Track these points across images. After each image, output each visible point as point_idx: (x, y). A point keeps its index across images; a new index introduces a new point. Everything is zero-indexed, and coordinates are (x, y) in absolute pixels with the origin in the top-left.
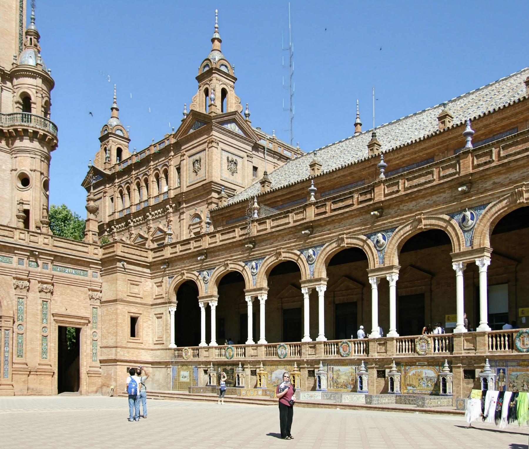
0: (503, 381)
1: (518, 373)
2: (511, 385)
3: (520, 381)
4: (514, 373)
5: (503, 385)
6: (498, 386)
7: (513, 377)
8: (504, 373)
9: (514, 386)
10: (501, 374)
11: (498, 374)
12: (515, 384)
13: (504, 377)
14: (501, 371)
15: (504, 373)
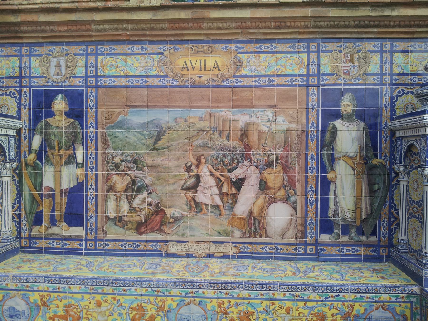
0: (71, 160)
1: (165, 117)
2: (120, 183)
3: (172, 161)
4: (137, 118)
5: (67, 183)
6: (38, 185)
7: (132, 137)
8: (76, 114)
9: (134, 188)
10: (60, 122)
11: (36, 118)
12: (147, 177)
13: (73, 139)
14: (59, 104)
15: (76, 114)
